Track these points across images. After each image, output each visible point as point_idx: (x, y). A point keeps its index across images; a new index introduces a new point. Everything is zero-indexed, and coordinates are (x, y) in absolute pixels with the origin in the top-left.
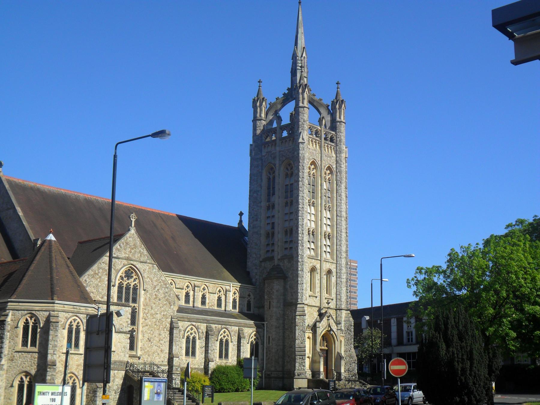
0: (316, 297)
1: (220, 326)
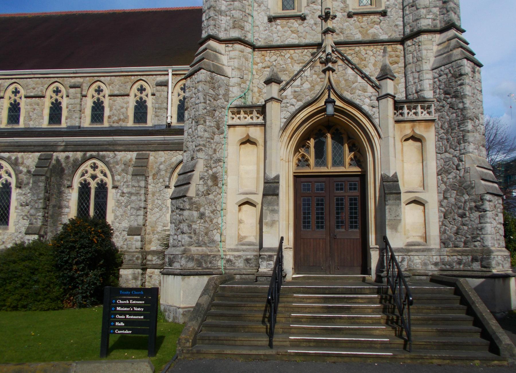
0: (303, 18)
1: (79, 155)
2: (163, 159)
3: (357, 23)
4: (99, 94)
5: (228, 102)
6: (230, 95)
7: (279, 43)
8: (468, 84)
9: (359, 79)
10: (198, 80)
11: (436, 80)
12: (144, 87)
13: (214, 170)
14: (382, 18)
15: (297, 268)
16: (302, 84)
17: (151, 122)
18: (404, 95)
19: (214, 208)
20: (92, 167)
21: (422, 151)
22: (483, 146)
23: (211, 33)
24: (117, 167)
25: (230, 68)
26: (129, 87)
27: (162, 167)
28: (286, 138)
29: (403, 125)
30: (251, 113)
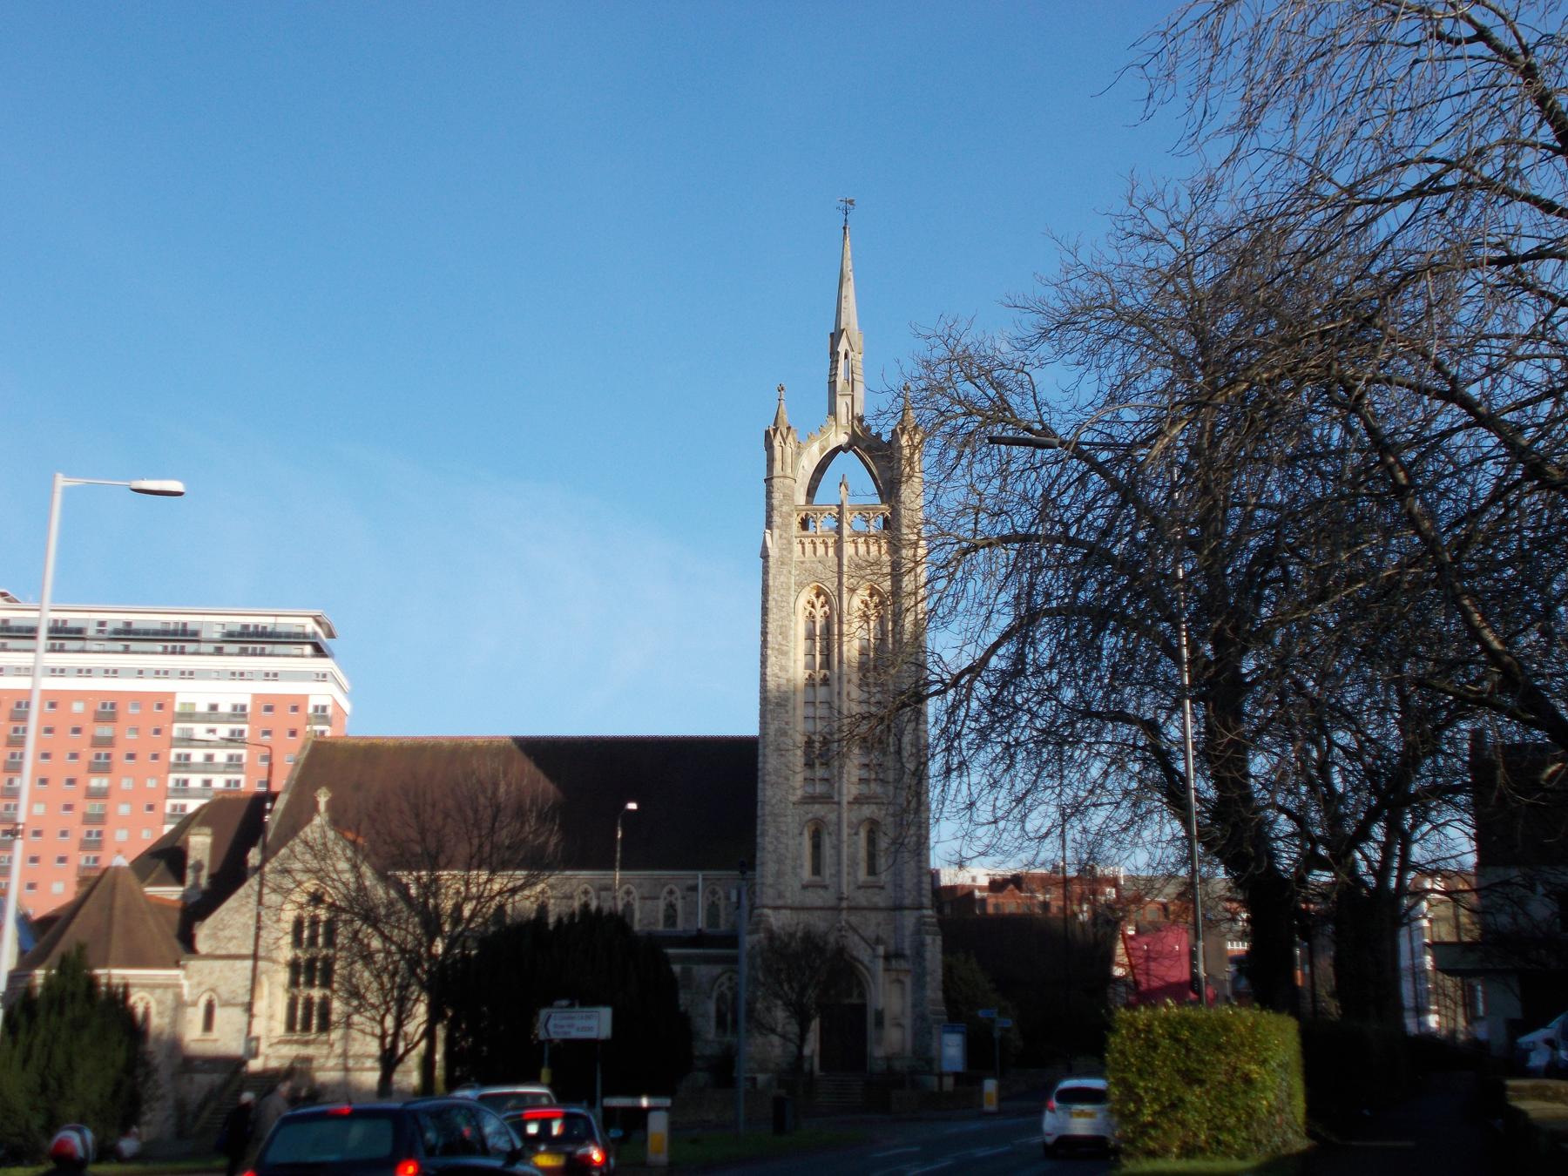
0: (825, 887)
15: (822, 1067)
17: (681, 925)
21: (903, 989)
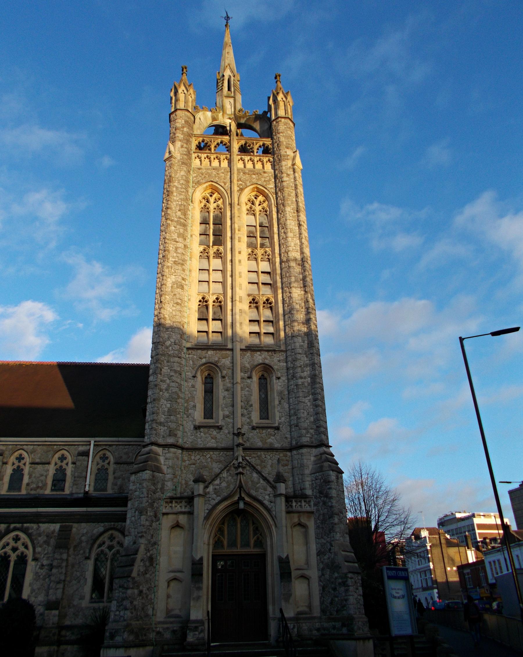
0: (220, 428)
2: (85, 531)
3: (259, 434)
4: (19, 462)
5: (163, 494)
6: (165, 488)
7: (202, 446)
8: (334, 489)
9: (262, 481)
10: (143, 478)
11: (314, 482)
12: (65, 456)
13: (151, 552)
14: (276, 431)
16: (220, 483)
18: (292, 490)
19: (150, 585)
20: (14, 539)
21: (306, 536)
22: (347, 534)
23: (153, 440)
24: (40, 538)
25: (166, 466)
26: (50, 456)
27: (83, 538)
28: (208, 526)
29: (292, 515)
30: (181, 502)
